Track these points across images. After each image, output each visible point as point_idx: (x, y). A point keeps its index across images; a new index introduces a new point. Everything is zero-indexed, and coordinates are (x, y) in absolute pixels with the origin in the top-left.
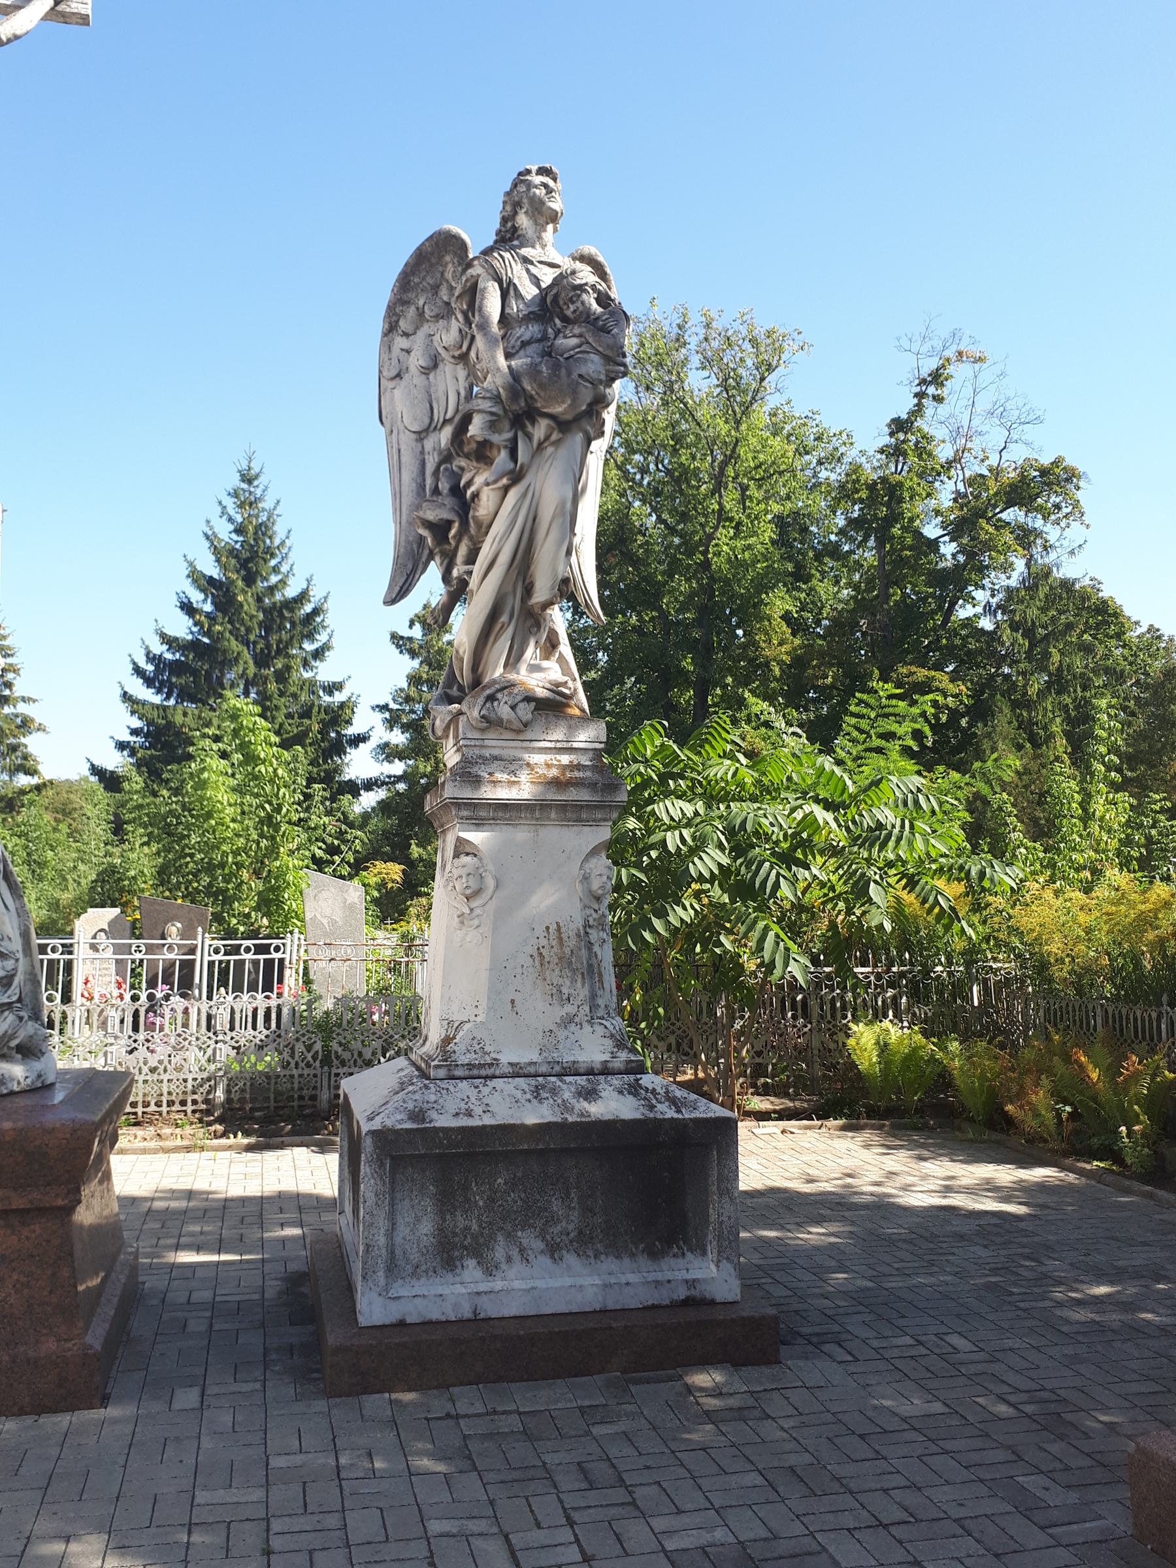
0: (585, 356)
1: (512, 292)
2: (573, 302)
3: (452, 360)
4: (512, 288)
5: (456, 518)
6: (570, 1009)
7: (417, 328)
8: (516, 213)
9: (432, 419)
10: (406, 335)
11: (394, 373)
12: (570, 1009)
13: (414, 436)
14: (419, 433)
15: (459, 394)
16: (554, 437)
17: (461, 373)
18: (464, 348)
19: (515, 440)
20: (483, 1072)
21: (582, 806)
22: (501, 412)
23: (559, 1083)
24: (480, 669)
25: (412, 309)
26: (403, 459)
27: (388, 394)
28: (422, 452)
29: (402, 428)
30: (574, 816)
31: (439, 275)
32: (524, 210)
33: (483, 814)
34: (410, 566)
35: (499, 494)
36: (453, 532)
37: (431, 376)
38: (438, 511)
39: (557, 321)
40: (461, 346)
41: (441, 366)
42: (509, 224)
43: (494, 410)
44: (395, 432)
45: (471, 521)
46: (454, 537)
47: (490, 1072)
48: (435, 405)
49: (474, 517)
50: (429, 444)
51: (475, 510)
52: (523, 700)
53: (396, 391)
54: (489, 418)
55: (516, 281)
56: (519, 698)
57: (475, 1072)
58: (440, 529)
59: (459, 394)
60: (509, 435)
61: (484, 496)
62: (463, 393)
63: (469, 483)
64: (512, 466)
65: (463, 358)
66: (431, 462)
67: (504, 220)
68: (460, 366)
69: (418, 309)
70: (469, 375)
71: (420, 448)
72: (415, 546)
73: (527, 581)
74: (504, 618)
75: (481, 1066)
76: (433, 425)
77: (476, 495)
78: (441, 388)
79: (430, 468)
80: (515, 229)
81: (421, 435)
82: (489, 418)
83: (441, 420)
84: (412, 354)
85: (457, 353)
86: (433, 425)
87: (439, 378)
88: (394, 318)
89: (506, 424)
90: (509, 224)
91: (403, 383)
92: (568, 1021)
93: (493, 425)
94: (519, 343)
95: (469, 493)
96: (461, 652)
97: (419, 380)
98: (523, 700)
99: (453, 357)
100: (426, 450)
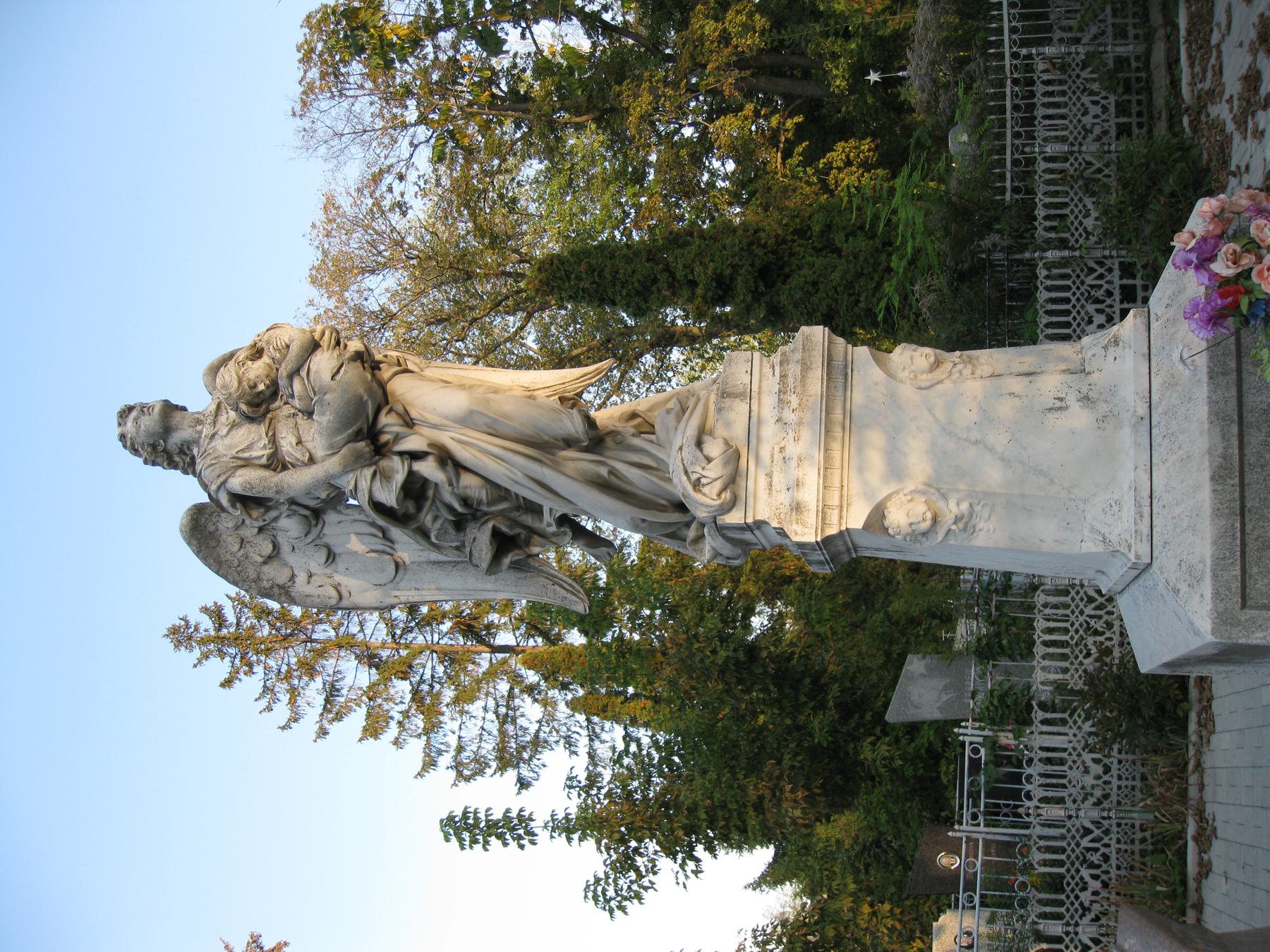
1: (246, 455)
2: (255, 386)
3: (320, 526)
4: (241, 455)
5: (490, 525)
6: (1071, 400)
7: (286, 565)
8: (165, 451)
9: (383, 552)
10: (293, 577)
11: (334, 593)
12: (1071, 400)
13: (401, 572)
16: (400, 408)
18: (307, 513)
19: (401, 454)
20: (1147, 502)
21: (829, 379)
22: (372, 470)
23: (1160, 410)
24: (664, 502)
25: (266, 569)
28: (419, 564)
29: (392, 585)
31: (230, 539)
32: (162, 439)
33: (834, 500)
37: (337, 550)
40: (306, 517)
41: (326, 540)
43: (369, 478)
45: (494, 509)
46: (510, 527)
47: (1146, 493)
49: (490, 504)
51: (480, 502)
52: (701, 450)
54: (377, 483)
55: (234, 452)
56: (698, 453)
57: (1146, 510)
58: (503, 543)
60: (396, 459)
64: (431, 459)
67: (172, 465)
69: (265, 563)
70: (335, 509)
73: (561, 444)
74: (604, 471)
75: (1138, 504)
76: (389, 550)
77: (465, 501)
79: (435, 556)
80: (182, 452)
82: (377, 483)
84: (313, 571)
85: (314, 522)
86: (389, 550)
88: (276, 590)
89: (384, 463)
92: (1086, 399)
93: (387, 477)
94: (300, 447)
95: (460, 509)
98: (701, 450)
99: (316, 525)
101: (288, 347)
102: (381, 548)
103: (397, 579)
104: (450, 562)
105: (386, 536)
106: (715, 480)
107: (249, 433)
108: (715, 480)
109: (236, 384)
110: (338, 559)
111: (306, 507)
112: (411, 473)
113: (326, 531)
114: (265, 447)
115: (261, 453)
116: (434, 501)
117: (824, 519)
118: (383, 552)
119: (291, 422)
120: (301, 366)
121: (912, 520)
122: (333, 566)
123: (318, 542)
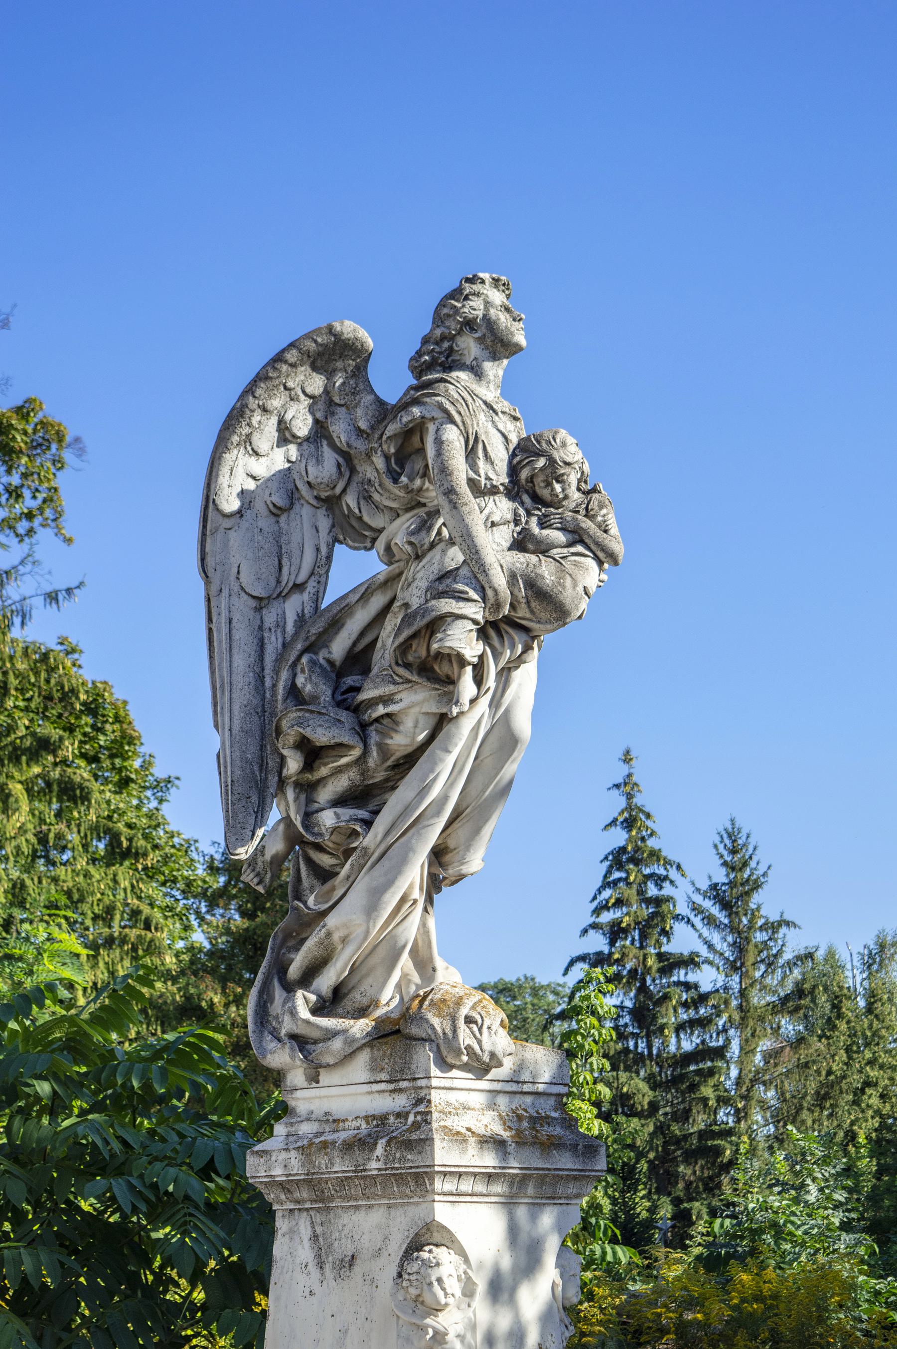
0: (582, 559)
1: (480, 453)
3: (314, 502)
4: (480, 446)
9: (278, 582)
13: (252, 603)
14: (260, 599)
15: (318, 550)
17: (324, 524)
18: (338, 490)
25: (274, 420)
26: (236, 635)
27: (219, 536)
28: (261, 628)
29: (236, 588)
30: (549, 1192)
34: (255, 799)
35: (432, 722)
36: (344, 761)
37: (283, 519)
38: (335, 731)
39: (526, 499)
41: (297, 507)
42: (446, 345)
44: (225, 593)
48: (285, 561)
49: (381, 746)
50: (270, 618)
51: (383, 734)
53: (232, 534)
59: (318, 550)
61: (408, 723)
62: (324, 550)
63: (386, 700)
65: (331, 503)
66: (273, 645)
68: (321, 512)
69: (281, 422)
70: (333, 526)
71: (259, 622)
72: (256, 768)
76: (278, 590)
78: (296, 538)
81: (261, 603)
83: (290, 584)
85: (324, 495)
87: (293, 524)
90: (446, 345)
91: (245, 524)
96: (336, 937)
97: (266, 522)
99: (317, 498)
100: (267, 625)
101: (606, 531)
102: (284, 578)
103: (245, 597)
104: (263, 669)
105: (298, 587)
106: (479, 1042)
107: (502, 460)
108: (479, 1042)
109: (568, 460)
110: (273, 519)
111: (344, 491)
112: (462, 662)
113: (306, 511)
114: (488, 478)
115: (483, 475)
116: (408, 681)
117: (452, 1173)
118: (278, 582)
119: (509, 516)
120: (588, 548)
121: (445, 1279)
122: (265, 512)
123: (296, 495)
